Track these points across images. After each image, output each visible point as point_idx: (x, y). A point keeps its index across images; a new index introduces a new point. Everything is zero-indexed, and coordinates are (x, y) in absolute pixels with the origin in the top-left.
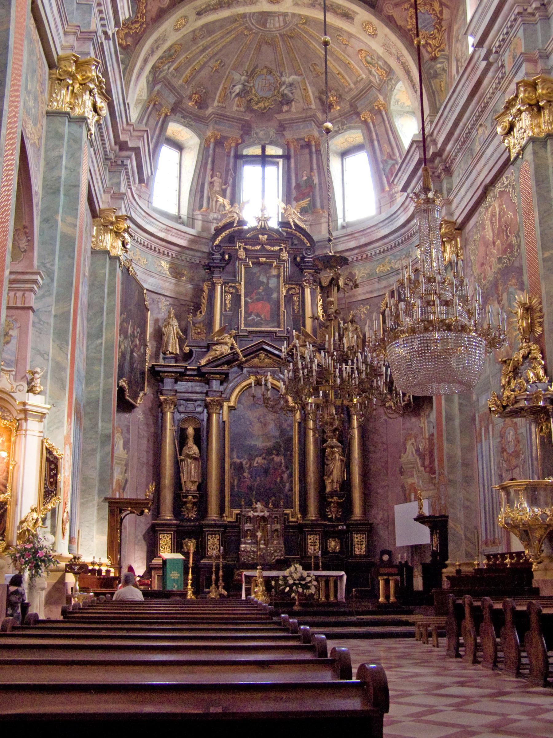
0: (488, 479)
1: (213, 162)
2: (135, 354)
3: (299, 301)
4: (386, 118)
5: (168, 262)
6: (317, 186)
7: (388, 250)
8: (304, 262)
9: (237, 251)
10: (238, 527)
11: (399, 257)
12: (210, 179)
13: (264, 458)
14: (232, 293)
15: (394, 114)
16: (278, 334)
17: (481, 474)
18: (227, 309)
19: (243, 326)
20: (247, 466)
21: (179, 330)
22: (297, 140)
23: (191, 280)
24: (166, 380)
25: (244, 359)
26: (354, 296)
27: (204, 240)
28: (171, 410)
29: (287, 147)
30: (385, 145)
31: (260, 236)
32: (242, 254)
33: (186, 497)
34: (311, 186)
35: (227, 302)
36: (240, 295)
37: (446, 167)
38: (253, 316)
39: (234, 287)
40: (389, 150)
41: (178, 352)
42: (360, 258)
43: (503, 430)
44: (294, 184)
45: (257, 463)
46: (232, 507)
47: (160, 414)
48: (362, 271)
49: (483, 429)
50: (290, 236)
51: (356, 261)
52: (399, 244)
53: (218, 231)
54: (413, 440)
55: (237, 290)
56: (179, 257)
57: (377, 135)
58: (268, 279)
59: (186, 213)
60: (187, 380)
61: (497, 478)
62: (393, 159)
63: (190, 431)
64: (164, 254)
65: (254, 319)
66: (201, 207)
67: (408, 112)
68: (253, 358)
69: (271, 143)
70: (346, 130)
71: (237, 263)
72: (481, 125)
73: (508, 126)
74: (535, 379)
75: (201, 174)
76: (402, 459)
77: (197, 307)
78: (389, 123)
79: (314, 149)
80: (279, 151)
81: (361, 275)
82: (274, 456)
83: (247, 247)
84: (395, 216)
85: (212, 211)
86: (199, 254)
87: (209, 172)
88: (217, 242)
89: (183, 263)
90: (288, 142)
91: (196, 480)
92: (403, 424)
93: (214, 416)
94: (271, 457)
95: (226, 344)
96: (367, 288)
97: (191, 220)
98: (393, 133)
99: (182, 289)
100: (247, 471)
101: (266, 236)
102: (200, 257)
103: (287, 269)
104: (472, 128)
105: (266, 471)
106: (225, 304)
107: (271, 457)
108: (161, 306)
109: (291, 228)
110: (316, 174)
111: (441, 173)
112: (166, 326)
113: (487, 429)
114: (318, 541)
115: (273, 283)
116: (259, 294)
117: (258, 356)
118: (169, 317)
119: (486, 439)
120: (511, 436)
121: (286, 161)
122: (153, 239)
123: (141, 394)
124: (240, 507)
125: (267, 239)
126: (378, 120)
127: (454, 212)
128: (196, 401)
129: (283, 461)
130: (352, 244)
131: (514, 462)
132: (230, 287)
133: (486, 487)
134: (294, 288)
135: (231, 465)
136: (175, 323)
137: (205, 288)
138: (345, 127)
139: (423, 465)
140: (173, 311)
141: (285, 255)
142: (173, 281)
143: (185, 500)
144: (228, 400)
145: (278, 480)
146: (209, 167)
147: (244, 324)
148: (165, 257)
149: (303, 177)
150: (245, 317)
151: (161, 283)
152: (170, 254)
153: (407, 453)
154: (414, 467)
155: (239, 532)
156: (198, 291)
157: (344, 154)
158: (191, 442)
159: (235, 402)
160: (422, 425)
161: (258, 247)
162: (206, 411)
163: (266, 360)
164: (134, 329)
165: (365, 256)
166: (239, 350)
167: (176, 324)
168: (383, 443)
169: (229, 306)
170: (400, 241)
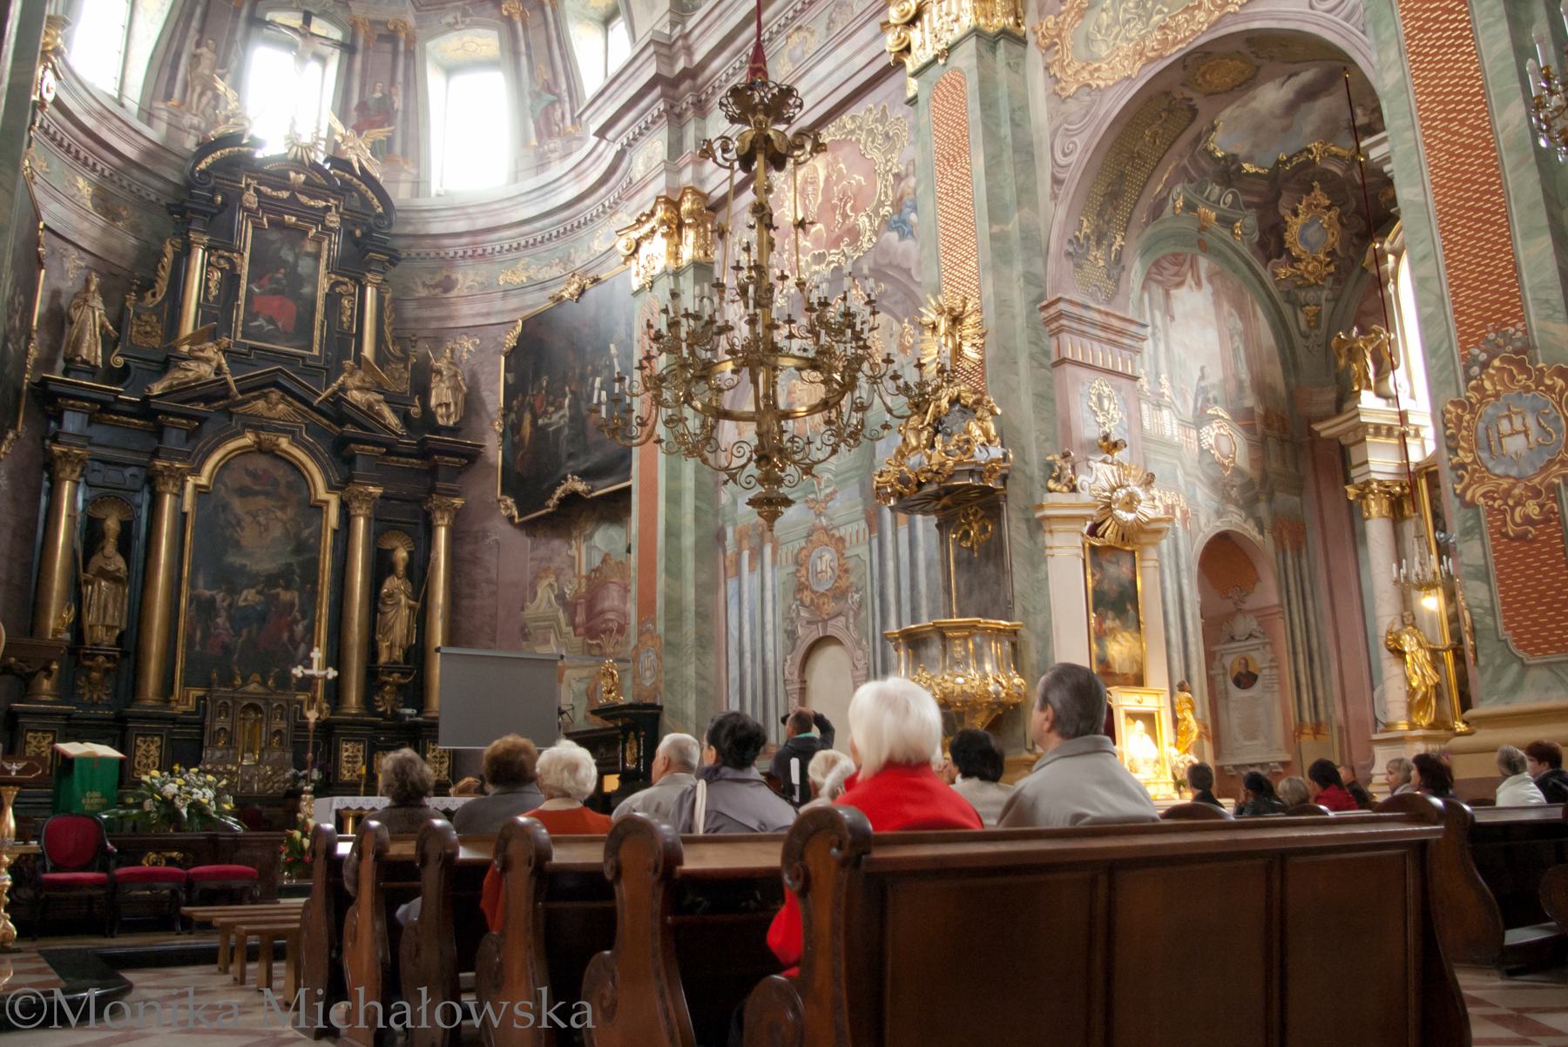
0: (753, 641)
1: (205, 16)
2: (10, 345)
3: (352, 309)
4: (551, 19)
5: (91, 183)
6: (400, 115)
7: (526, 247)
8: (371, 238)
9: (241, 192)
10: (201, 725)
11: (544, 263)
12: (193, 48)
13: (259, 593)
14: (221, 270)
15: (569, 14)
16: (309, 362)
17: (734, 632)
18: (211, 298)
19: (239, 335)
20: (225, 604)
21: (105, 319)
22: (374, 23)
23: (135, 229)
24: (68, 416)
25: (240, 397)
26: (450, 318)
27: (173, 158)
28: (75, 476)
29: (352, 29)
30: (542, 66)
31: (292, 175)
32: (251, 199)
33: (93, 657)
34: (388, 113)
35: (211, 284)
36: (239, 276)
37: (700, 101)
38: (260, 322)
39: (229, 260)
40: (548, 76)
41: (100, 360)
42: (470, 253)
43: (805, 552)
44: (355, 101)
45: (246, 600)
46: (187, 684)
47: (46, 484)
48: (471, 277)
49: (746, 554)
50: (347, 188)
51: (463, 257)
52: (550, 239)
53: (206, 147)
54: (552, 579)
55: (233, 265)
56: (115, 178)
57: (528, 46)
58: (297, 257)
59: (138, 100)
60: (115, 425)
61: (781, 636)
62: (553, 94)
63: (112, 524)
64: (85, 164)
65: (261, 326)
66: (168, 96)
67: (591, 19)
68: (255, 398)
69: (320, 16)
70: (469, 26)
71: (240, 216)
72: (799, 28)
73: (913, 11)
74: (982, 439)
75: (178, 34)
76: (527, 612)
77: (148, 285)
78: (557, 28)
79: (402, 47)
80: (337, 35)
81: (469, 283)
82: (279, 590)
83: (262, 188)
84: (558, 184)
85: (189, 110)
86: (159, 184)
87: (193, 35)
88: (203, 166)
89: (121, 193)
90: (355, 22)
91: (117, 623)
92: (532, 550)
93: (168, 501)
94: (273, 591)
95: (208, 361)
96: (480, 307)
97: (145, 115)
98: (560, 47)
99: (114, 243)
100: (223, 614)
101: (302, 177)
102: (159, 190)
103: (333, 246)
104: (778, 32)
105: (263, 618)
106: (207, 287)
107: (273, 591)
108: (68, 265)
109: (352, 172)
110: (401, 93)
111: (686, 109)
112: (78, 307)
113: (757, 554)
114: (361, 754)
115: (304, 266)
116: (278, 281)
117: (265, 396)
118: (87, 289)
119: (752, 570)
120: (825, 560)
121: (346, 56)
122: (69, 125)
123: (11, 435)
124: (208, 685)
125: (304, 183)
126: (536, 18)
127: (707, 178)
128: (126, 466)
129: (297, 601)
130: (461, 226)
131: (830, 607)
132: (221, 257)
133: (748, 656)
134: (345, 284)
135: (190, 604)
136: (97, 303)
137: (169, 249)
138: (468, 20)
139: (572, 623)
140: (95, 280)
141: (333, 220)
142: (99, 220)
143: (88, 663)
144: (197, 471)
145: (285, 636)
146: (195, 24)
147: (243, 332)
148: (86, 171)
149: (374, 91)
150: (244, 321)
151: (74, 219)
152: (98, 168)
153: (537, 601)
154: (551, 627)
155: (202, 735)
156: (149, 257)
157: (450, 70)
158: (110, 547)
159: (210, 477)
160: (574, 552)
161: (285, 194)
162: (146, 489)
163: (281, 406)
164: (15, 293)
165: (480, 251)
166: (230, 379)
167: (101, 306)
168: (489, 582)
169: (214, 292)
170: (554, 233)
